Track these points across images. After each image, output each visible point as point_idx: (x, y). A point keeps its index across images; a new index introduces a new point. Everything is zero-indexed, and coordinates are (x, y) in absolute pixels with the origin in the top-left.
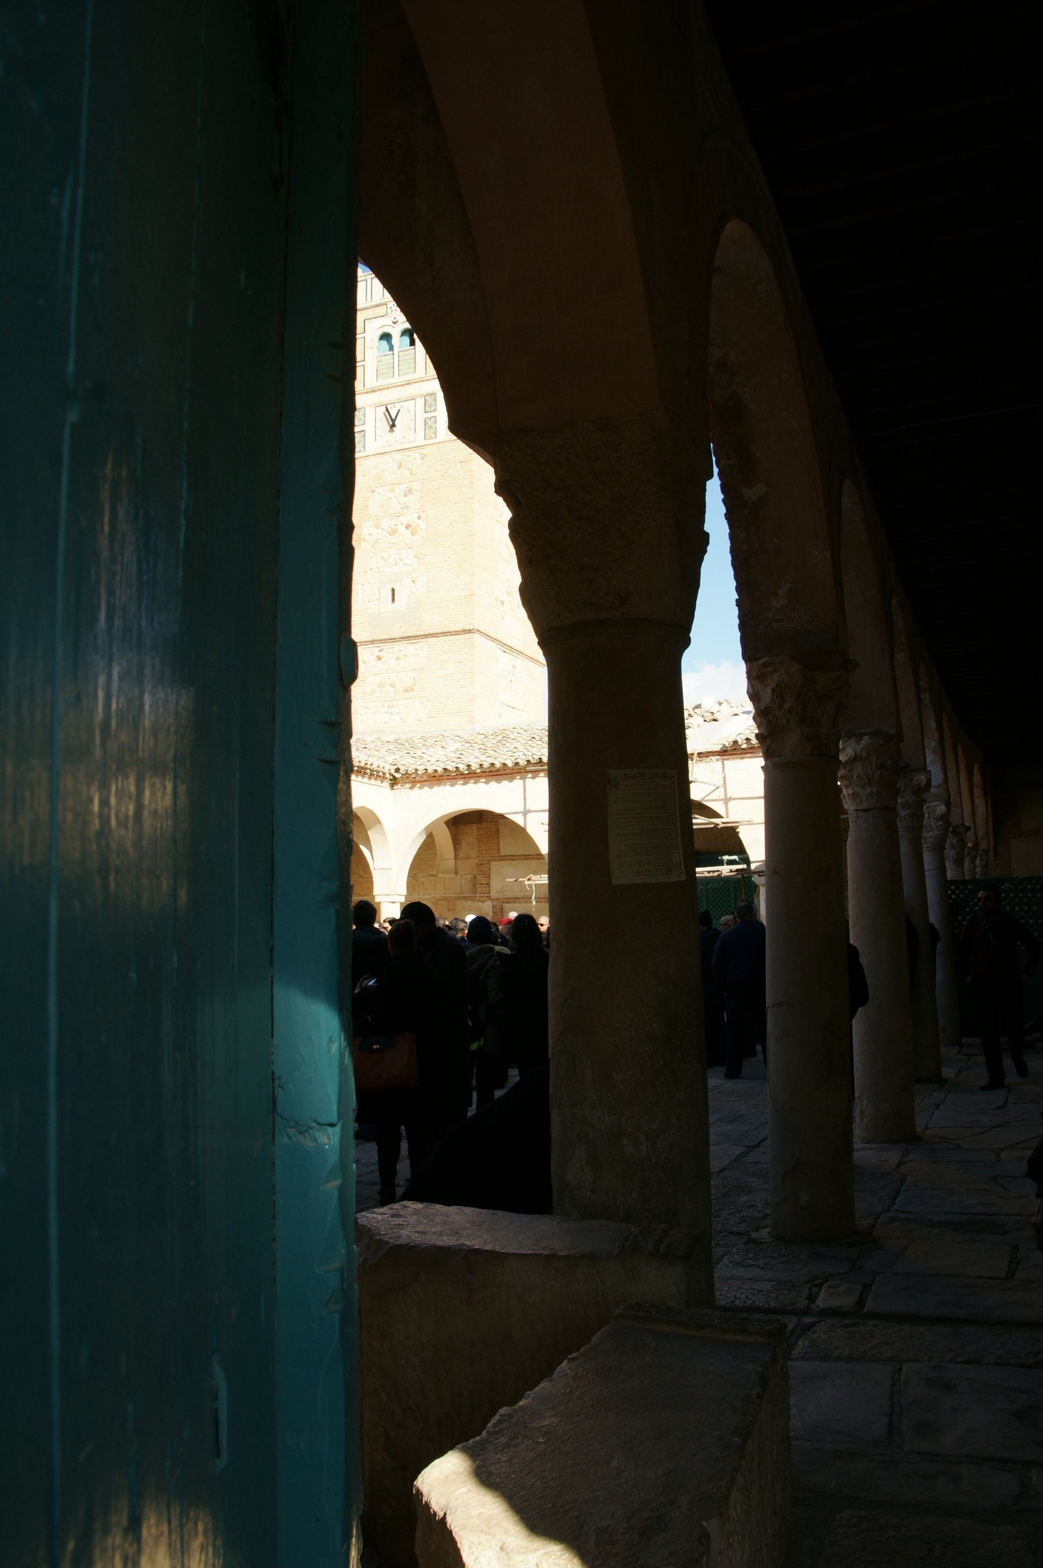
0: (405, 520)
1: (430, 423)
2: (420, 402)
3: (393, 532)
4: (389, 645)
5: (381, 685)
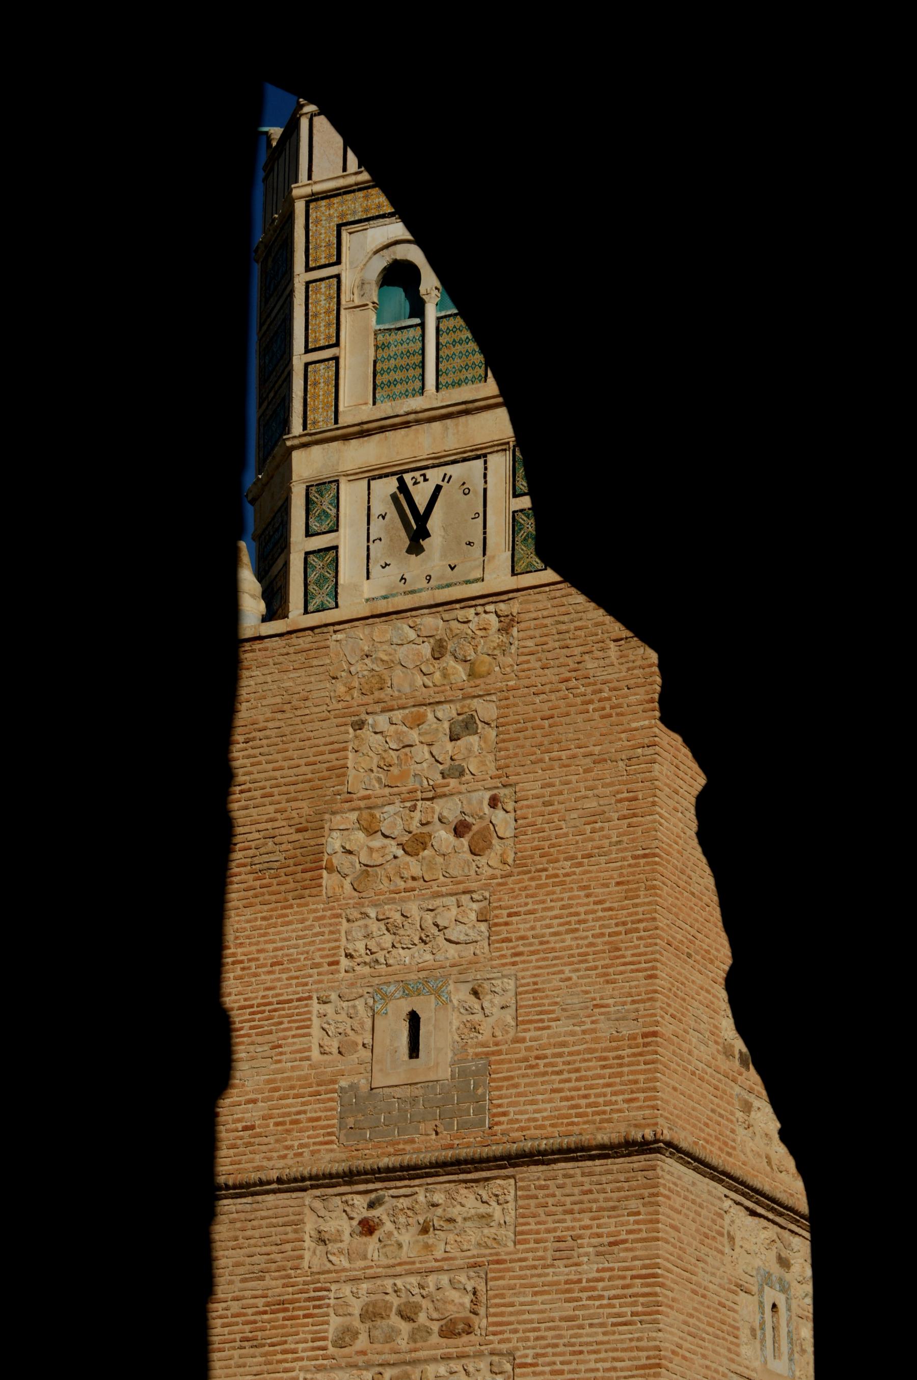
0: (450, 809)
3: (416, 844)
4: (402, 1187)
5: (371, 1314)
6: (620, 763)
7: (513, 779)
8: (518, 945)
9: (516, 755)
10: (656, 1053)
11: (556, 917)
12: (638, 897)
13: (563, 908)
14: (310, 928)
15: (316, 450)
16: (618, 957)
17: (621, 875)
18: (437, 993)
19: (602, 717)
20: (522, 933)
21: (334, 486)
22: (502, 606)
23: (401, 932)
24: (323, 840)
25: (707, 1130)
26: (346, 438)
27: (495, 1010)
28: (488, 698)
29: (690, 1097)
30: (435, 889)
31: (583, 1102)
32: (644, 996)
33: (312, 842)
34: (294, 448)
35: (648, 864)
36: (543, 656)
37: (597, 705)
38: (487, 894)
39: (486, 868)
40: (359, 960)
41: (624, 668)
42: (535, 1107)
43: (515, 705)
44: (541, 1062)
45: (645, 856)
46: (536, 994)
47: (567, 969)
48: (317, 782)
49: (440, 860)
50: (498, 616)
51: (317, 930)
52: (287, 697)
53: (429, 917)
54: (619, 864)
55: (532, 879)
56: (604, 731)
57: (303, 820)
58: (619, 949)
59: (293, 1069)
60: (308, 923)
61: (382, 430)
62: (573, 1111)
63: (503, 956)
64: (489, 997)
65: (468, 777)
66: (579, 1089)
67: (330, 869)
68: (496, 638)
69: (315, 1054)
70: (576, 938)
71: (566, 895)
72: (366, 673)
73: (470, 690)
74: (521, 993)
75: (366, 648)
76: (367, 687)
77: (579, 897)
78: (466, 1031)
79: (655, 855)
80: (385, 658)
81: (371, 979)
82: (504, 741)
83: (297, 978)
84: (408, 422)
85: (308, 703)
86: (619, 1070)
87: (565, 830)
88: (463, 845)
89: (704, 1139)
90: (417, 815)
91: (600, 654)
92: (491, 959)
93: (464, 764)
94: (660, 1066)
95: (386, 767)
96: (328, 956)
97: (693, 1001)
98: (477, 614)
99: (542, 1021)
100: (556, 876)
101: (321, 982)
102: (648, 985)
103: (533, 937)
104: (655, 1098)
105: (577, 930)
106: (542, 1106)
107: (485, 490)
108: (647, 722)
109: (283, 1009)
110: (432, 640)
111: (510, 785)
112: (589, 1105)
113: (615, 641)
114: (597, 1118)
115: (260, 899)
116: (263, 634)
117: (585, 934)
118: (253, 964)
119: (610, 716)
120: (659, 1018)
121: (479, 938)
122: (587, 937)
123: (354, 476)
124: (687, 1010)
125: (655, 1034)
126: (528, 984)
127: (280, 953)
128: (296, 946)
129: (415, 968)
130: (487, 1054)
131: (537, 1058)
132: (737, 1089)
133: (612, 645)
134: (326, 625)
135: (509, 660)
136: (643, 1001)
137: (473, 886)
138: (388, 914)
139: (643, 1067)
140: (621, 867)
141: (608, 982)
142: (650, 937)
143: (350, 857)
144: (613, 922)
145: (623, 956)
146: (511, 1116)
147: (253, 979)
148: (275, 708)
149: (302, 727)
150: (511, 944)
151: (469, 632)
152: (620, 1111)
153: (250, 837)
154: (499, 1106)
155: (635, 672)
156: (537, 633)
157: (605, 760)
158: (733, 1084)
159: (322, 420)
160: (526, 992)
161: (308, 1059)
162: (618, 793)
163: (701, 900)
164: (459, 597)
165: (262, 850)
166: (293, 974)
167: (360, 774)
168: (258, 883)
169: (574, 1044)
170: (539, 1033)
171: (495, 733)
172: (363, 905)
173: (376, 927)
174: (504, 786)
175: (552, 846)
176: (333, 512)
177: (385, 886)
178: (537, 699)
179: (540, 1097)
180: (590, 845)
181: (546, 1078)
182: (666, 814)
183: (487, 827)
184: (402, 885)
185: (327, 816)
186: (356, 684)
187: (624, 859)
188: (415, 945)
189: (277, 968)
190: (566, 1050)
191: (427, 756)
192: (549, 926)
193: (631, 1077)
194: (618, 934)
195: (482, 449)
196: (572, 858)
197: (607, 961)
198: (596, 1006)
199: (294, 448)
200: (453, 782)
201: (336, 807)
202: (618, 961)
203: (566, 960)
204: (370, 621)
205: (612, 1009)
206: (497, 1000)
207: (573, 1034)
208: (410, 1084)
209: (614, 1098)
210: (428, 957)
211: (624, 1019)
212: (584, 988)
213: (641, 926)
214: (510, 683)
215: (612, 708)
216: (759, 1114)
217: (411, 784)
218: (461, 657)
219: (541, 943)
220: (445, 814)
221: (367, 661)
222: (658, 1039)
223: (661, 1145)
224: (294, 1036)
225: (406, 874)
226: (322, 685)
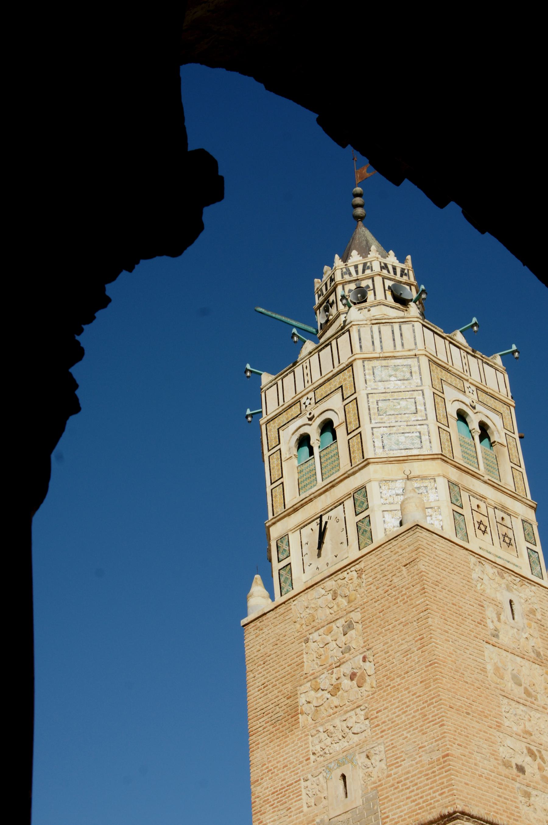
0: (346, 669)
1: (363, 526)
2: (349, 503)
3: (335, 690)
6: (415, 623)
7: (371, 645)
8: (382, 727)
9: (371, 633)
10: (449, 765)
11: (397, 707)
12: (430, 686)
13: (399, 702)
14: (296, 745)
15: (278, 524)
16: (426, 720)
17: (422, 677)
18: (351, 761)
19: (404, 603)
20: (383, 720)
21: (286, 537)
22: (357, 566)
23: (334, 735)
24: (298, 700)
25: (495, 806)
26: (289, 515)
27: (378, 763)
28: (356, 611)
29: (479, 788)
30: (345, 709)
31: (421, 801)
32: (440, 737)
33: (294, 702)
34: (270, 526)
35: (433, 668)
36: (376, 583)
37: (401, 598)
38: (367, 705)
39: (365, 692)
40: (318, 755)
41: (410, 577)
42: (400, 809)
43: (368, 610)
44: (400, 785)
45: (431, 665)
46: (394, 749)
47: (405, 732)
48: (293, 673)
49: (345, 694)
50: (356, 571)
51: (299, 744)
52: (278, 637)
53: (344, 724)
54: (420, 672)
55: (384, 691)
56: (405, 610)
57: (289, 693)
58: (425, 716)
59: (297, 819)
60: (295, 742)
61: (302, 506)
62: (417, 807)
63: (377, 734)
64: (374, 757)
65: (353, 650)
66: (418, 794)
67: (302, 713)
68: (356, 581)
69: (305, 808)
70: (407, 715)
71: (400, 695)
72: (307, 616)
73: (349, 609)
74: (387, 751)
75: (306, 604)
76: (308, 622)
77: (405, 694)
78: (366, 778)
79: (435, 663)
80: (313, 606)
81: (324, 763)
82: (365, 628)
83: (294, 771)
84: (311, 499)
85: (286, 637)
86: (435, 779)
87: (395, 663)
88: (354, 684)
89: (494, 812)
90: (335, 676)
91: (400, 574)
92: (372, 737)
93: (350, 645)
94: (452, 771)
95: (319, 657)
96: (305, 756)
97: (475, 737)
98: (348, 573)
99: (397, 762)
100: (394, 687)
101: (303, 770)
102: (441, 730)
103: (389, 720)
104: (453, 790)
105: (407, 711)
106: (403, 808)
107: (345, 517)
108: (423, 600)
109: (290, 789)
110: (331, 592)
111: (370, 649)
112: (424, 802)
113: (405, 566)
114: (428, 808)
115: (276, 736)
116: (266, 611)
117: (410, 712)
118: (276, 770)
119: (407, 602)
120: (448, 746)
121: (366, 728)
122: (411, 713)
123: (293, 530)
124: (470, 741)
125: (447, 755)
126: (389, 745)
127: (286, 761)
128: (292, 756)
129: (341, 752)
130: (376, 787)
131: (398, 783)
132: (518, 785)
133: (404, 568)
134: (289, 599)
135: (363, 590)
136: (440, 739)
137: (360, 703)
138: (327, 728)
139: (445, 774)
140: (421, 674)
141: (423, 734)
142: (438, 705)
143: (309, 704)
144: (421, 702)
145: (428, 719)
146: (391, 817)
147: (276, 777)
148: (274, 644)
149: (285, 649)
150: (380, 727)
151: (346, 583)
152: (438, 801)
153: (269, 708)
154: (385, 813)
155: (415, 577)
156: (372, 573)
157: (408, 624)
158: (513, 782)
159: (279, 510)
160: (389, 750)
161: (302, 812)
162: (415, 637)
163: (473, 685)
164: (339, 568)
165: (274, 713)
166: (292, 769)
167: (310, 665)
168: (274, 729)
169: (413, 771)
170: (397, 769)
171: (361, 626)
172: (316, 727)
173: (323, 736)
174: (368, 650)
175: (391, 672)
176: (287, 549)
177: (325, 714)
178: (376, 604)
179: (402, 803)
180: (406, 667)
181: (403, 792)
182: (440, 643)
183: (363, 672)
184: (331, 711)
185: (298, 688)
186: (304, 622)
187: (422, 669)
188: (340, 740)
189: (285, 769)
190: (410, 775)
191: (335, 646)
192: (394, 713)
193: (440, 781)
194: (424, 708)
195: (341, 500)
196: (400, 676)
197: (422, 723)
198: (420, 748)
199: (270, 526)
200: (347, 655)
201: (301, 682)
202: (426, 722)
203: (404, 728)
204: (306, 591)
205: (427, 747)
206: (378, 758)
207: (412, 766)
208: (345, 812)
209: (434, 795)
210: (346, 744)
211: (433, 751)
212: (414, 740)
213: (434, 700)
214: (364, 601)
215: (407, 598)
216: (537, 799)
217: (330, 661)
218: (343, 595)
219: (392, 723)
220: (345, 671)
221: (307, 610)
222: (450, 757)
223: (458, 814)
224: (295, 802)
225: (333, 706)
226: (290, 627)
